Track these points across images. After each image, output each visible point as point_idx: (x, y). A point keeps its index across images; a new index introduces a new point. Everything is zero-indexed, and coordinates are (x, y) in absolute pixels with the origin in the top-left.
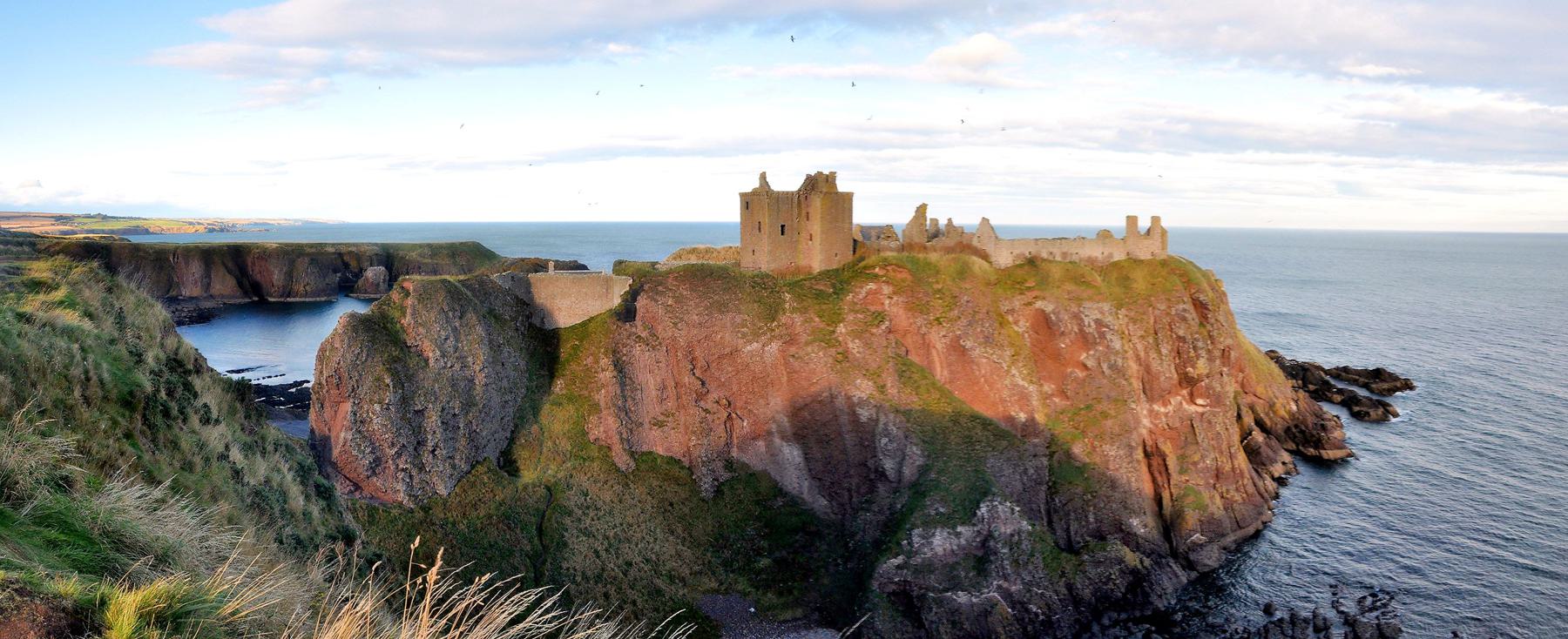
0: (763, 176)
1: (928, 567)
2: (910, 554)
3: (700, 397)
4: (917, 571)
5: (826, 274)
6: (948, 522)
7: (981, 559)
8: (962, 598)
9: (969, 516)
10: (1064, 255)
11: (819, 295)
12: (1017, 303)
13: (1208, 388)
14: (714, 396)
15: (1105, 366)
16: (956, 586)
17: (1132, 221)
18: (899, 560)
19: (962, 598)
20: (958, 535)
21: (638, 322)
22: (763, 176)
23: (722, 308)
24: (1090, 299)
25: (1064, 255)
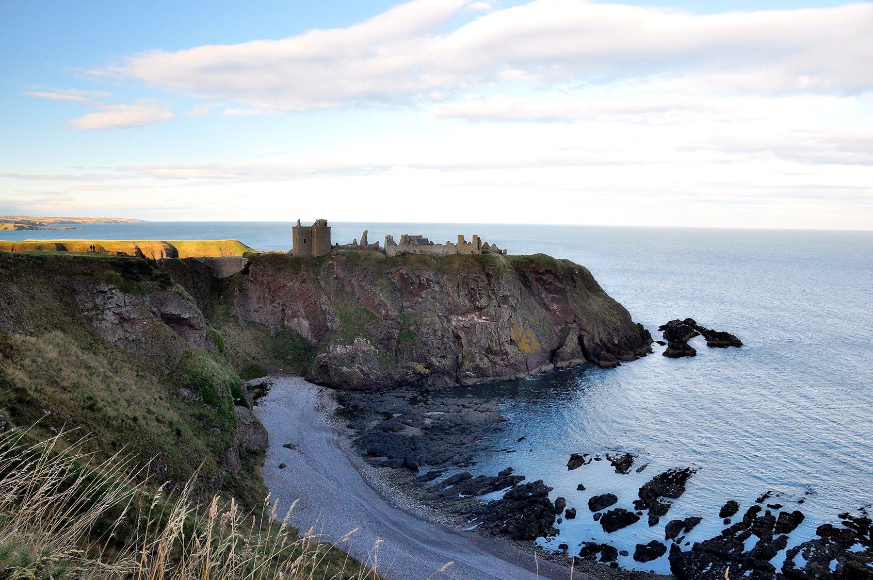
0: (299, 221)
1: (335, 358)
2: (328, 353)
3: (272, 302)
4: (330, 359)
5: (318, 257)
6: (343, 344)
7: (352, 358)
8: (345, 369)
9: (351, 343)
10: (421, 251)
11: (315, 265)
12: (393, 270)
13: (487, 312)
14: (277, 302)
15: (429, 297)
16: (343, 365)
17: (461, 237)
18: (325, 354)
19: (345, 369)
20: (346, 348)
21: (250, 275)
22: (299, 221)
23: (280, 269)
24: (425, 270)
25: (421, 251)
